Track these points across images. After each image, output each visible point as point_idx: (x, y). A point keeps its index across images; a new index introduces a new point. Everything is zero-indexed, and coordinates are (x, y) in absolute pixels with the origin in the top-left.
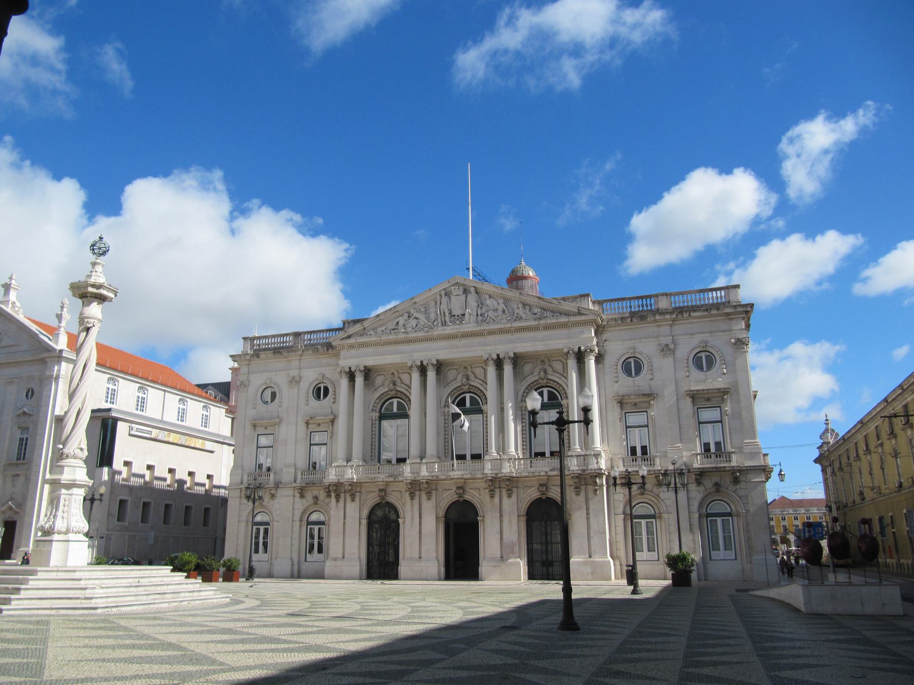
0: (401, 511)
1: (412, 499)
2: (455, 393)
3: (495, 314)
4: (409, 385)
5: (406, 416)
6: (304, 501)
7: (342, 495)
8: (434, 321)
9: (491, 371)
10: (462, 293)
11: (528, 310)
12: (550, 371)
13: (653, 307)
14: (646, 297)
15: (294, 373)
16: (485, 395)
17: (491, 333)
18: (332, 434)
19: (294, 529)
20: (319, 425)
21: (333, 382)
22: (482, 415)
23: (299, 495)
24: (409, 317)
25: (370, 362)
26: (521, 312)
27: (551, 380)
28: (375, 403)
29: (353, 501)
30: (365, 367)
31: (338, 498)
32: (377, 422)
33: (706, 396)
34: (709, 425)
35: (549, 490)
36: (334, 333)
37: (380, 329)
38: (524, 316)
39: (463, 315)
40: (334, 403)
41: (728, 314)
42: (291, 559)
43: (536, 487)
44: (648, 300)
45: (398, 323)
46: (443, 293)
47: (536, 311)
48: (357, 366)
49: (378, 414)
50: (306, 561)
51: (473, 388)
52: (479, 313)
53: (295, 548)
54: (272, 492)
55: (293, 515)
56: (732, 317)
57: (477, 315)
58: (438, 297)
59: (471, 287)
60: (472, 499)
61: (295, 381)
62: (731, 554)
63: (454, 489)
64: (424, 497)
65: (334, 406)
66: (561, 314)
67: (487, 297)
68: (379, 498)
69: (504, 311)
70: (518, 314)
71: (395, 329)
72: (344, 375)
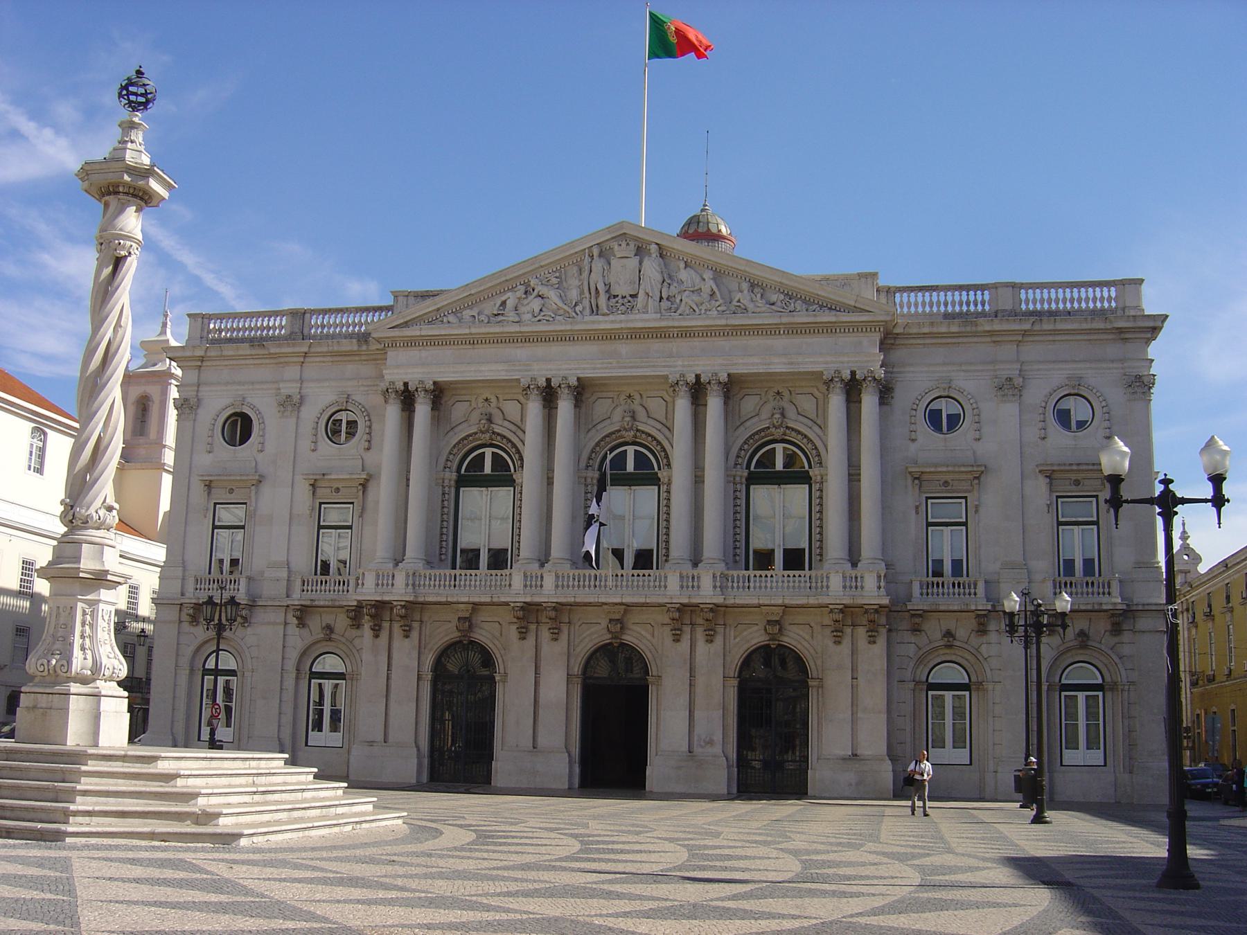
1: (523, 635)
3: (695, 298)
4: (519, 423)
5: (509, 481)
6: (305, 632)
7: (386, 625)
8: (575, 305)
9: (682, 406)
10: (634, 253)
11: (759, 295)
12: (791, 413)
13: (987, 308)
14: (976, 288)
15: (290, 388)
16: (664, 450)
17: (686, 333)
18: (363, 509)
19: (286, 684)
20: (338, 490)
21: (366, 410)
22: (656, 487)
23: (295, 621)
24: (526, 293)
25: (446, 375)
26: (744, 297)
27: (793, 429)
28: (450, 453)
29: (407, 637)
31: (376, 631)
32: (453, 490)
33: (1073, 476)
34: (1075, 527)
35: (785, 632)
36: (377, 314)
37: (467, 313)
38: (750, 306)
39: (634, 296)
41: (1120, 330)
42: (279, 740)
43: (761, 626)
44: (979, 293)
45: (504, 303)
46: (596, 252)
47: (774, 298)
48: (421, 382)
49: (454, 476)
50: (306, 745)
51: (644, 436)
53: (287, 719)
54: (244, 613)
55: (283, 658)
56: (1127, 336)
57: (661, 298)
58: (587, 259)
59: (650, 243)
61: (291, 404)
62: (1096, 757)
63: (604, 623)
64: (545, 634)
65: (368, 457)
66: (821, 307)
67: (682, 265)
68: (458, 634)
69: (712, 294)
70: (739, 301)
72: (393, 395)
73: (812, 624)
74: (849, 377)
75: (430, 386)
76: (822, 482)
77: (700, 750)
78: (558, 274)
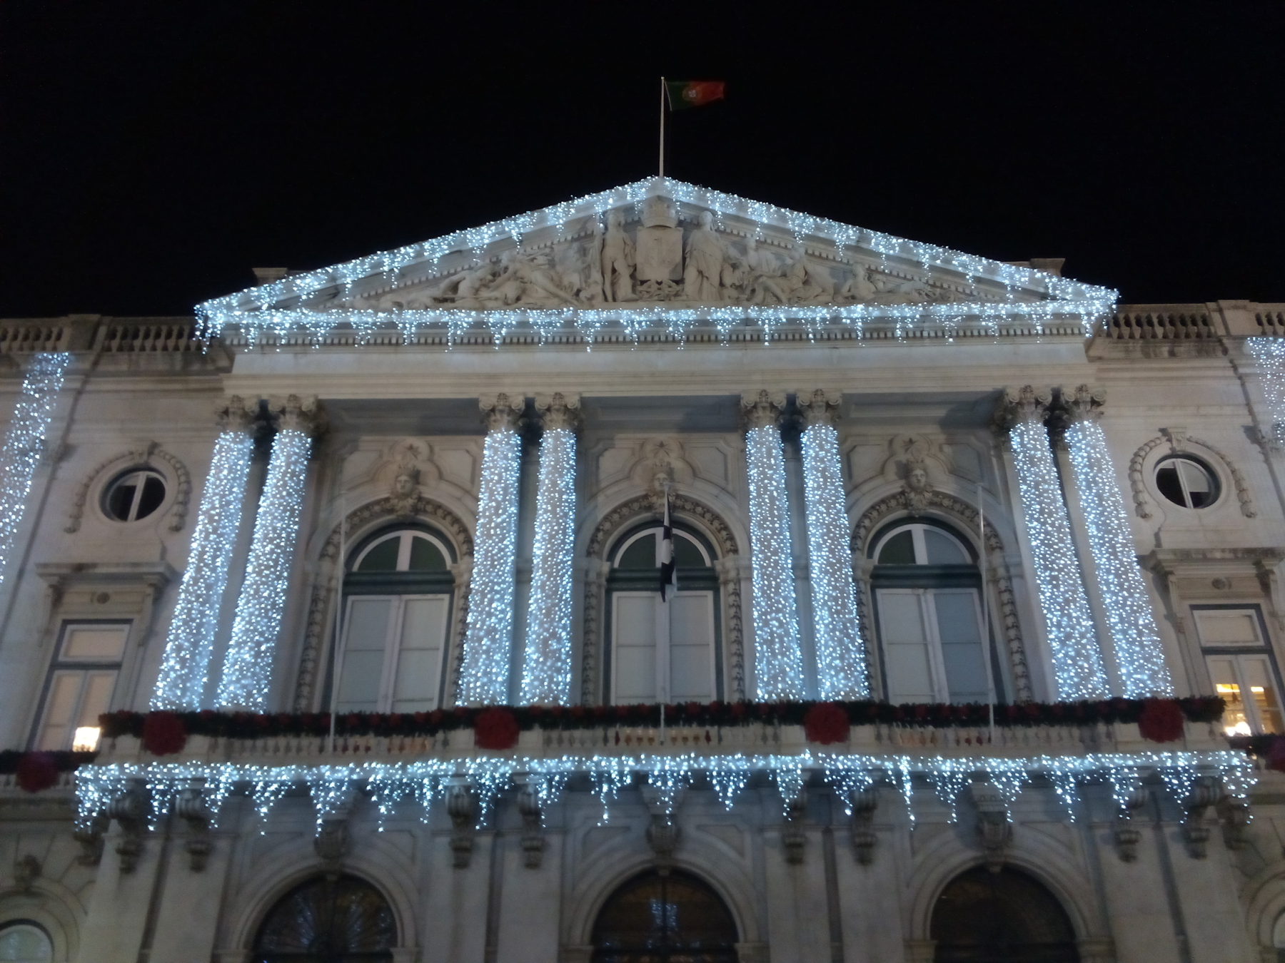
2: (623, 518)
4: (468, 486)
21: (184, 467)
22: (710, 594)
29: (198, 867)
57: (722, 284)
64: (513, 860)
76: (1009, 579)
78: (547, 250)
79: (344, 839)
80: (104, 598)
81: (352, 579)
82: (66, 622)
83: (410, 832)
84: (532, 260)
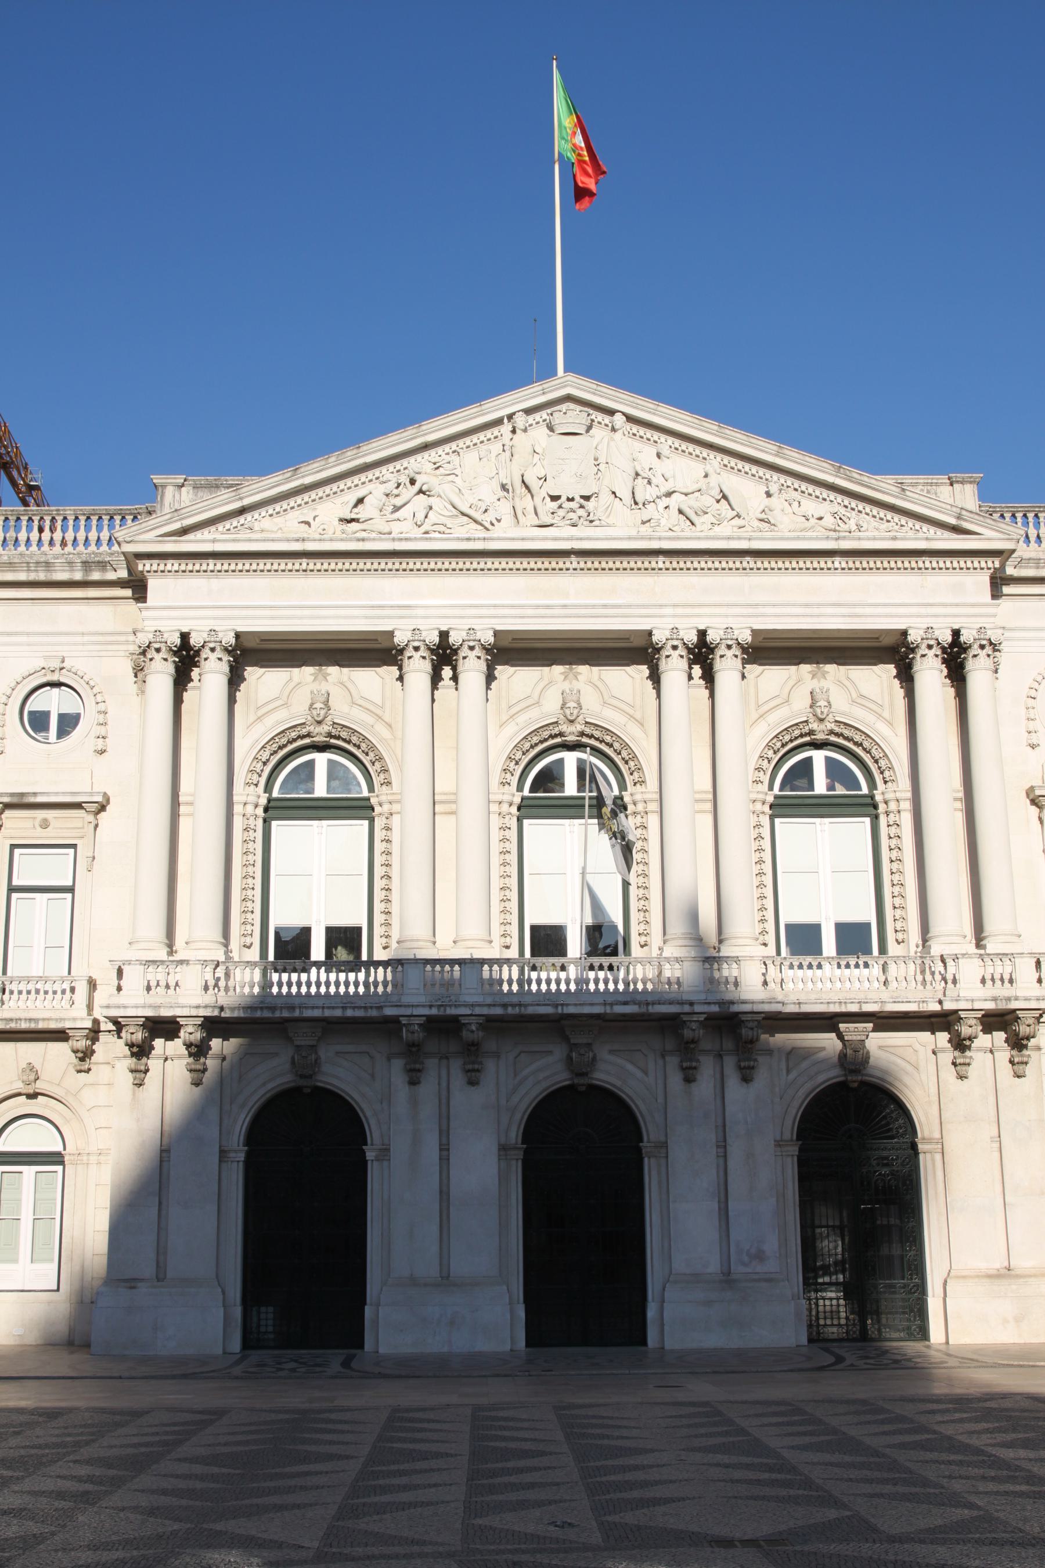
0: (373, 1122)
11: (796, 504)
30: (238, 636)
40: (102, 752)
45: (360, 501)
52: (639, 498)
60: (618, 1083)
64: (458, 1079)
71: (353, 520)
73: (917, 1047)
74: (950, 639)
75: (230, 639)
77: (742, 1269)
79: (316, 1060)
80: (45, 824)
81: (272, 804)
82: (13, 847)
83: (368, 1053)
84: (437, 468)
